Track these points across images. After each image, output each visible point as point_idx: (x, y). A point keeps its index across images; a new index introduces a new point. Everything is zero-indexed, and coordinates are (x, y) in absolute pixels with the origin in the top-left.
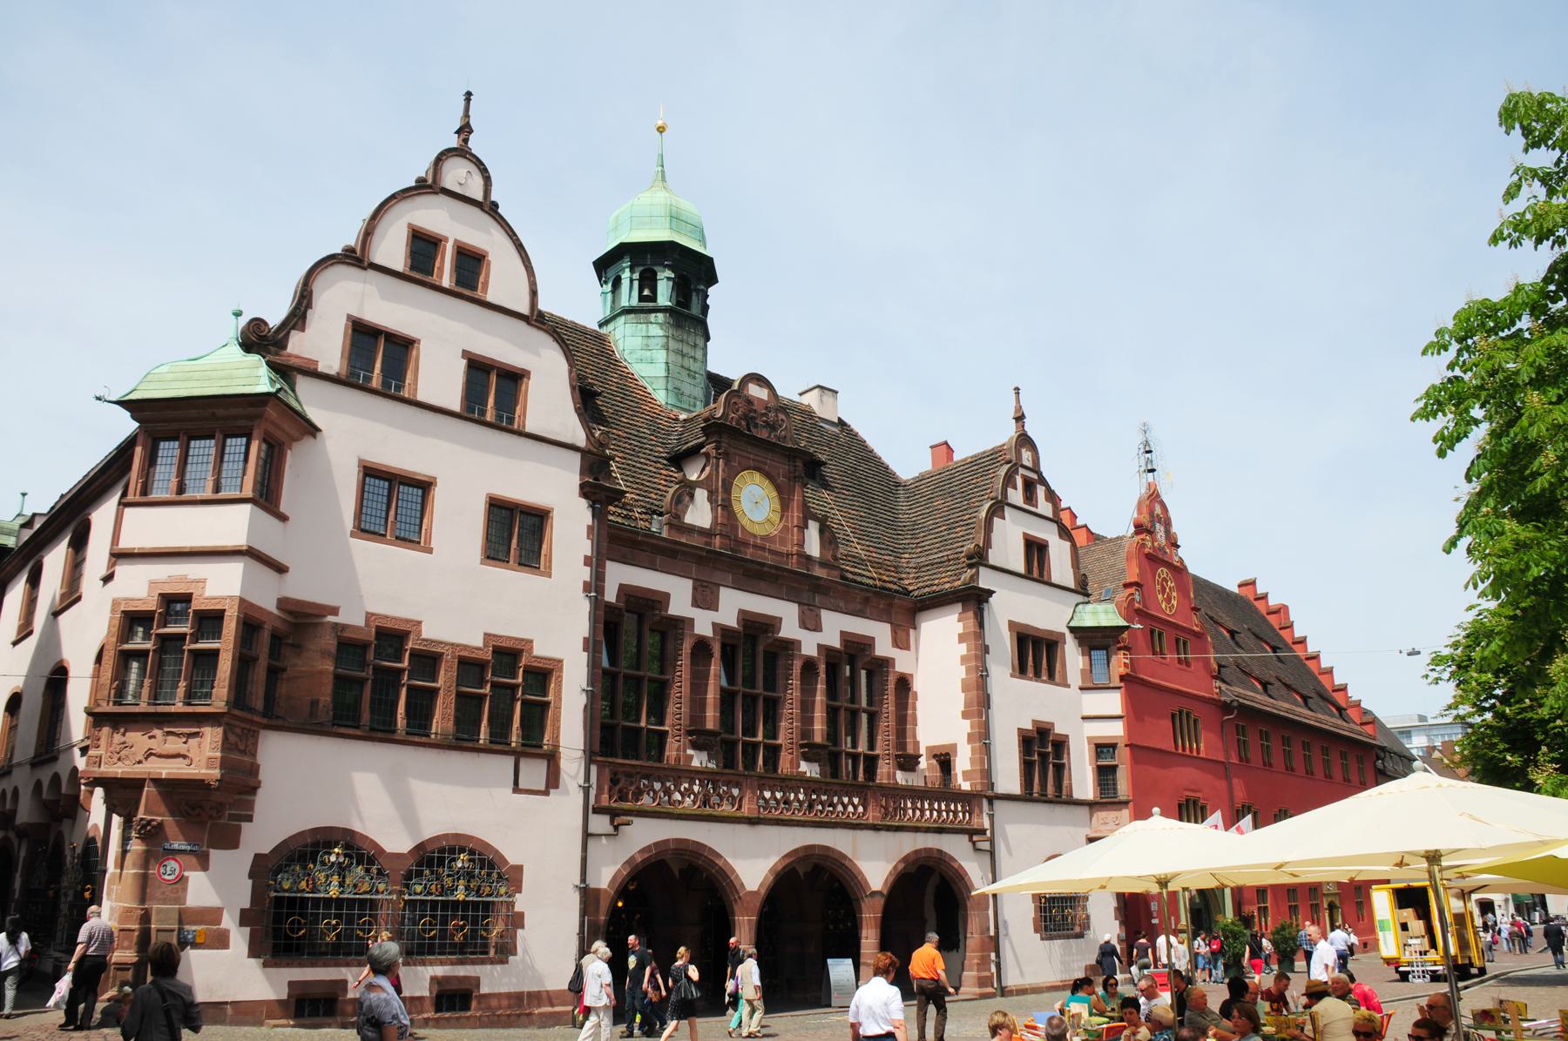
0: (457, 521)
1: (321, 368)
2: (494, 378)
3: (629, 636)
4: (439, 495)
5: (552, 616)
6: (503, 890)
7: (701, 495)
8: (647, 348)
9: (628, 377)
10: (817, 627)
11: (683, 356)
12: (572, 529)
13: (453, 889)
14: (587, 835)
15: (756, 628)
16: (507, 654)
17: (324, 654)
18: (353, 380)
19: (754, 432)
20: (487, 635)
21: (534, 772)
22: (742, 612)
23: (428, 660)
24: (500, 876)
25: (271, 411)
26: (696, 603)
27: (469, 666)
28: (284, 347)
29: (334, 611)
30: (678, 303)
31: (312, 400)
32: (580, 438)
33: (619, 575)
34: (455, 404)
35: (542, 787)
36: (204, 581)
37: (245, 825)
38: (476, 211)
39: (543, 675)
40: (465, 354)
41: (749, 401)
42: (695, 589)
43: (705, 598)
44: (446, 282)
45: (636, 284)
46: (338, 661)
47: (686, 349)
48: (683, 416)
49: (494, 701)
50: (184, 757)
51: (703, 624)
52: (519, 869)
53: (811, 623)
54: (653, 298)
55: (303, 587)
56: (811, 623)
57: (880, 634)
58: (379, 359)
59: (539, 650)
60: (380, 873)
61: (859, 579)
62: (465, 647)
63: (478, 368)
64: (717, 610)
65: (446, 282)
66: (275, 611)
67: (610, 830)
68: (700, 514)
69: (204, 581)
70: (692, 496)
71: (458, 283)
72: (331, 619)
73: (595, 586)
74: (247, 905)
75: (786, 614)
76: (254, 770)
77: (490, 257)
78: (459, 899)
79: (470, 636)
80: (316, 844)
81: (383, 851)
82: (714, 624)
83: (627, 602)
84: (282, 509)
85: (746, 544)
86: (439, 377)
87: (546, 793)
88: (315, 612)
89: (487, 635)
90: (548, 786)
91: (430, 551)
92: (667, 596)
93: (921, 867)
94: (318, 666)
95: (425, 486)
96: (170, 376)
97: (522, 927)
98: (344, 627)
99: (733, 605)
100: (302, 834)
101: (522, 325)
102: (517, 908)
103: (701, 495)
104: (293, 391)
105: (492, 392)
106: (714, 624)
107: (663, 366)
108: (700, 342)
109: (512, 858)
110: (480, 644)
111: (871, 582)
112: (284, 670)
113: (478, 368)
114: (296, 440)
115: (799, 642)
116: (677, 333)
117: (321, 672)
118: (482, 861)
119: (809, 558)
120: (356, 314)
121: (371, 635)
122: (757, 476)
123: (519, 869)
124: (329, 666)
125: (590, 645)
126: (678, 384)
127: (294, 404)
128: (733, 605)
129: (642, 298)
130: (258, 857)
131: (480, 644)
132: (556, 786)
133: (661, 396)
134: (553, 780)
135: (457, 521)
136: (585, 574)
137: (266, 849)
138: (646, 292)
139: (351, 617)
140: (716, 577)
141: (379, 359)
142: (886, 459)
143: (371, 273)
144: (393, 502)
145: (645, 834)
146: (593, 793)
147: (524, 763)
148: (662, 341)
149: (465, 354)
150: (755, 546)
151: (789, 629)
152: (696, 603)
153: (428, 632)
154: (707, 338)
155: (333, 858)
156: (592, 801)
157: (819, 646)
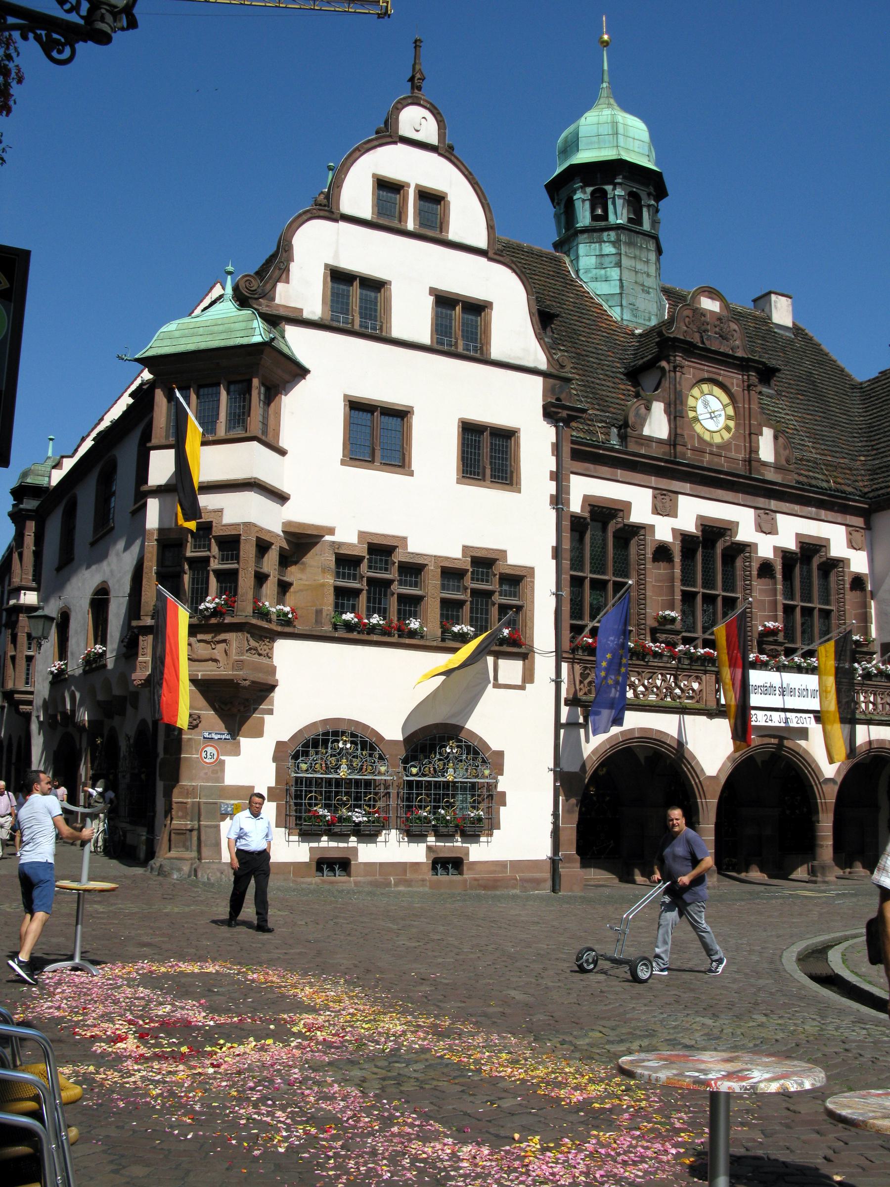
0: (435, 445)
1: (306, 315)
2: (458, 309)
3: (595, 541)
4: (418, 424)
5: (521, 526)
6: (487, 772)
7: (658, 408)
8: (601, 266)
9: (585, 295)
11: (636, 272)
12: (537, 446)
15: (713, 533)
16: (484, 563)
17: (324, 570)
18: (335, 324)
19: (708, 344)
20: (465, 548)
22: (700, 518)
23: (413, 570)
24: (484, 761)
25: (267, 359)
26: (656, 511)
27: (451, 574)
28: (273, 299)
29: (331, 531)
30: (630, 220)
31: (298, 342)
32: (540, 360)
33: (583, 488)
34: (425, 338)
35: (519, 683)
36: (221, 511)
37: (267, 718)
38: (434, 156)
39: (517, 580)
40: (433, 291)
41: (703, 313)
42: (655, 497)
43: (664, 506)
44: (410, 225)
45: (587, 204)
46: (338, 575)
47: (640, 266)
48: (638, 332)
50: (216, 661)
51: (664, 530)
52: (500, 754)
53: (767, 527)
54: (605, 217)
55: (301, 511)
56: (767, 527)
57: (835, 536)
58: (357, 304)
59: (512, 560)
60: (381, 758)
61: (814, 482)
62: (447, 558)
63: (444, 301)
64: (676, 517)
65: (410, 225)
66: (281, 534)
68: (657, 425)
69: (221, 511)
70: (648, 409)
71: (422, 225)
72: (328, 538)
73: (559, 500)
74: (273, 784)
76: (273, 670)
77: (449, 198)
79: (450, 549)
80: (326, 734)
81: (381, 738)
82: (674, 530)
83: (591, 512)
84: (283, 443)
86: (412, 316)
87: (522, 688)
88: (315, 533)
89: (465, 548)
90: (525, 680)
91: (411, 474)
92: (629, 504)
93: (876, 757)
95: (402, 415)
96: (177, 334)
97: (504, 805)
98: (340, 545)
99: (692, 511)
100: (314, 724)
101: (483, 260)
102: (500, 788)
103: (658, 408)
104: (283, 337)
105: (460, 326)
106: (674, 530)
107: (618, 283)
108: (653, 256)
109: (495, 746)
110: (459, 555)
111: (825, 485)
112: (291, 584)
113: (444, 301)
114: (288, 382)
115: (756, 545)
116: (632, 251)
117: (323, 585)
118: (468, 747)
119: (765, 464)
120: (331, 262)
121: (363, 551)
123: (500, 754)
124: (330, 580)
125: (557, 553)
126: (632, 300)
127: (285, 350)
128: (692, 511)
129: (595, 218)
130: (279, 744)
131: (459, 555)
132: (531, 681)
133: (615, 313)
134: (528, 677)
135: (435, 445)
137: (285, 738)
138: (599, 212)
139: (347, 535)
140: (676, 485)
141: (357, 304)
142: (841, 363)
143: (342, 225)
144: (377, 433)
146: (564, 687)
147: (501, 662)
148: (614, 259)
149: (433, 291)
151: (746, 532)
152: (656, 511)
153: (411, 549)
154: (659, 251)
155: (341, 745)
156: (564, 694)
157: (776, 549)
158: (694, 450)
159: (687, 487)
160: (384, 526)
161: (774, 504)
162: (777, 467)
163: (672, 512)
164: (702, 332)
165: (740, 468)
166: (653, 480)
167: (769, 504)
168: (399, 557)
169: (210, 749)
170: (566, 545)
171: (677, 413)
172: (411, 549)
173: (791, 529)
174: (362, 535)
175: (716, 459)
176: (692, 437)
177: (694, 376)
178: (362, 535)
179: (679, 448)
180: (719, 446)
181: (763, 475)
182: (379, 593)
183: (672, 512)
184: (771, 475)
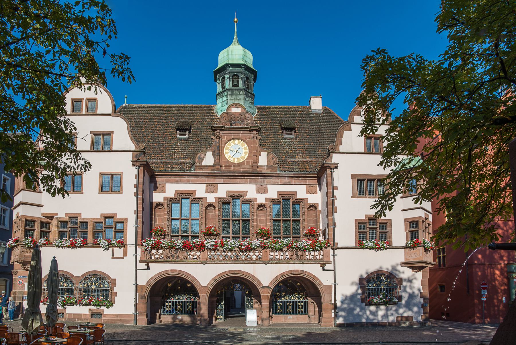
5: (124, 205)
7: (209, 154)
10: (266, 191)
12: (130, 176)
13: (91, 285)
14: (136, 270)
20: (101, 214)
21: (119, 252)
23: (85, 223)
26: (207, 192)
29: (57, 214)
41: (232, 114)
42: (207, 187)
49: (104, 232)
51: (211, 198)
67: (146, 268)
68: (209, 159)
70: (205, 155)
75: (250, 190)
78: (99, 289)
79: (97, 216)
82: (215, 198)
85: (230, 166)
87: (123, 258)
92: (195, 191)
94: (54, 229)
98: (60, 218)
99: (223, 189)
103: (209, 154)
106: (215, 198)
110: (100, 217)
119: (261, 167)
122: (236, 141)
125: (136, 212)
128: (223, 189)
131: (100, 217)
134: (125, 254)
136: (135, 190)
139: (62, 215)
140: (217, 180)
145: (158, 269)
150: (234, 166)
152: (207, 192)
153: (82, 217)
158: (226, 166)
159: (222, 180)
160: (73, 211)
161: (266, 181)
162: (268, 167)
163: (215, 191)
164: (231, 121)
165: (249, 170)
166: (206, 180)
167: (264, 181)
168: (79, 220)
169: (20, 281)
170: (140, 209)
171: (218, 153)
172: (82, 217)
173: (274, 190)
174: (66, 214)
175: (236, 169)
176: (225, 162)
177: (227, 139)
178: (66, 214)
179: (217, 167)
180: (237, 164)
181: (261, 171)
182: (75, 232)
183: (215, 191)
184: (265, 171)
